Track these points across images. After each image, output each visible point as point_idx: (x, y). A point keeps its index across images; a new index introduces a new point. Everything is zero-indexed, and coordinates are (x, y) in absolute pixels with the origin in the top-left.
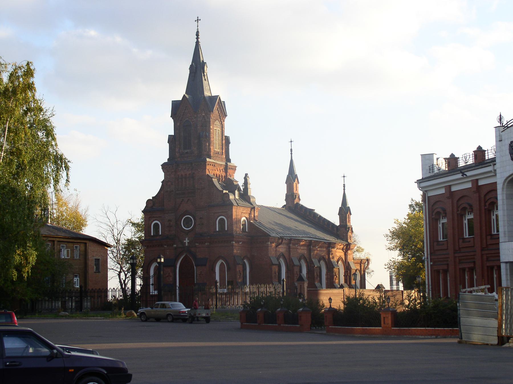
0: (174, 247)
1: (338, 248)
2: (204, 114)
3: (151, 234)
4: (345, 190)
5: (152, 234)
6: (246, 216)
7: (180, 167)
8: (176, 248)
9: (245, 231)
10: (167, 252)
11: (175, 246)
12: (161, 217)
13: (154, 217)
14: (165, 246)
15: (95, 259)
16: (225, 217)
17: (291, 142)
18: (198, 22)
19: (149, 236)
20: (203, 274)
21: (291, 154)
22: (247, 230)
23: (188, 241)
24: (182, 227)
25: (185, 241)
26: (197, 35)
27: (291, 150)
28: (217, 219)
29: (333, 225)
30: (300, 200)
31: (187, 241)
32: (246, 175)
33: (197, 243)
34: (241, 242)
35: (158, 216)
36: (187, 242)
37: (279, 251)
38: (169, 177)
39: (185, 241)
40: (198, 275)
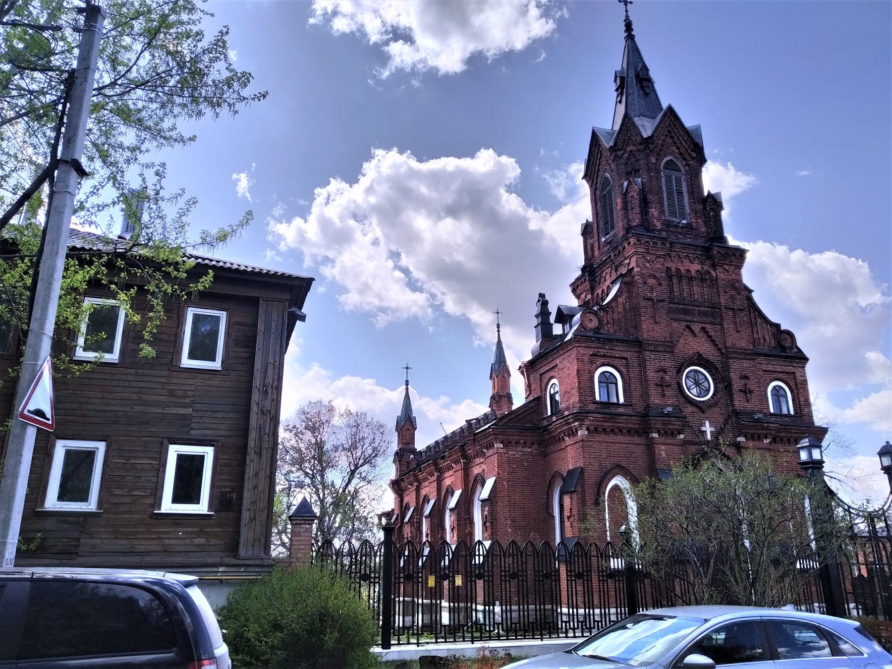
7: (675, 251)
8: (685, 443)
11: (682, 436)
12: (626, 359)
13: (604, 356)
23: (713, 429)
26: (629, 26)
35: (617, 355)
38: (648, 265)
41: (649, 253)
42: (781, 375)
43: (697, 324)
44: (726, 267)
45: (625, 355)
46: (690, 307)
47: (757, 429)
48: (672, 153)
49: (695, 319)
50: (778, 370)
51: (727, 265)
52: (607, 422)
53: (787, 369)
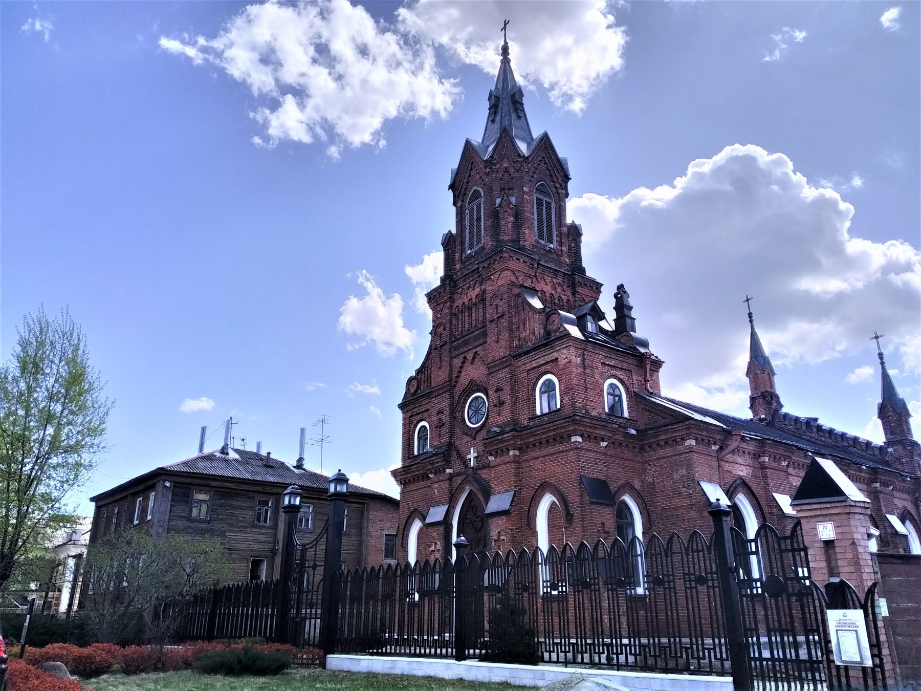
0: (448, 474)
1: (896, 488)
2: (506, 165)
3: (413, 454)
4: (886, 365)
5: (416, 453)
6: (621, 377)
8: (451, 477)
9: (622, 417)
10: (436, 490)
11: (448, 471)
12: (428, 410)
13: (417, 414)
14: (430, 475)
15: (386, 535)
16: (551, 373)
17: (748, 300)
18: (505, 30)
19: (409, 458)
20: (504, 540)
21: (751, 321)
22: (626, 415)
23: (476, 455)
24: (465, 422)
25: (468, 457)
27: (750, 315)
28: (535, 385)
29: (868, 444)
30: (782, 406)
31: (472, 455)
32: (621, 287)
33: (491, 455)
34: (603, 440)
35: (423, 410)
36: (474, 457)
37: (731, 472)
38: (439, 316)
39: (468, 457)
40: (493, 543)
41: (439, 304)
42: (548, 367)
43: (470, 352)
44: (492, 277)
45: (428, 407)
46: (468, 337)
47: (496, 444)
48: (476, 184)
49: (470, 348)
50: (541, 363)
51: (493, 274)
52: (408, 473)
53: (550, 358)
